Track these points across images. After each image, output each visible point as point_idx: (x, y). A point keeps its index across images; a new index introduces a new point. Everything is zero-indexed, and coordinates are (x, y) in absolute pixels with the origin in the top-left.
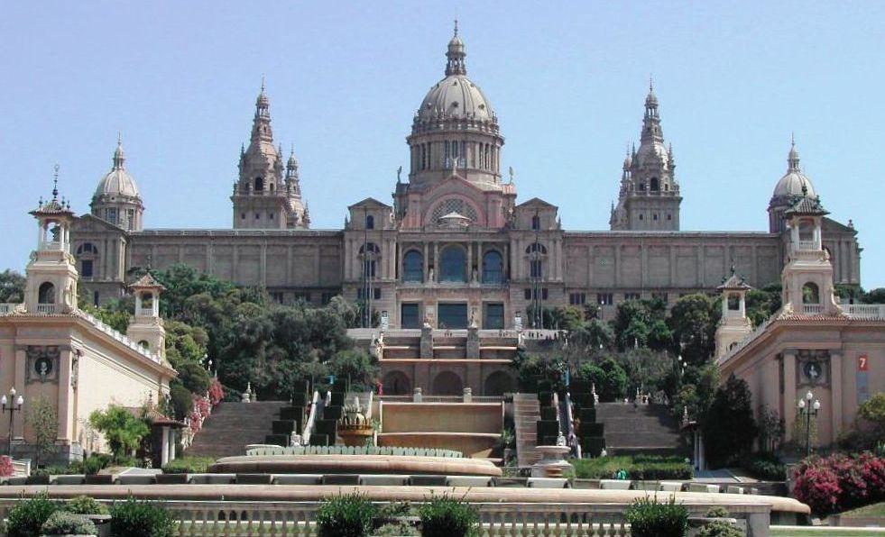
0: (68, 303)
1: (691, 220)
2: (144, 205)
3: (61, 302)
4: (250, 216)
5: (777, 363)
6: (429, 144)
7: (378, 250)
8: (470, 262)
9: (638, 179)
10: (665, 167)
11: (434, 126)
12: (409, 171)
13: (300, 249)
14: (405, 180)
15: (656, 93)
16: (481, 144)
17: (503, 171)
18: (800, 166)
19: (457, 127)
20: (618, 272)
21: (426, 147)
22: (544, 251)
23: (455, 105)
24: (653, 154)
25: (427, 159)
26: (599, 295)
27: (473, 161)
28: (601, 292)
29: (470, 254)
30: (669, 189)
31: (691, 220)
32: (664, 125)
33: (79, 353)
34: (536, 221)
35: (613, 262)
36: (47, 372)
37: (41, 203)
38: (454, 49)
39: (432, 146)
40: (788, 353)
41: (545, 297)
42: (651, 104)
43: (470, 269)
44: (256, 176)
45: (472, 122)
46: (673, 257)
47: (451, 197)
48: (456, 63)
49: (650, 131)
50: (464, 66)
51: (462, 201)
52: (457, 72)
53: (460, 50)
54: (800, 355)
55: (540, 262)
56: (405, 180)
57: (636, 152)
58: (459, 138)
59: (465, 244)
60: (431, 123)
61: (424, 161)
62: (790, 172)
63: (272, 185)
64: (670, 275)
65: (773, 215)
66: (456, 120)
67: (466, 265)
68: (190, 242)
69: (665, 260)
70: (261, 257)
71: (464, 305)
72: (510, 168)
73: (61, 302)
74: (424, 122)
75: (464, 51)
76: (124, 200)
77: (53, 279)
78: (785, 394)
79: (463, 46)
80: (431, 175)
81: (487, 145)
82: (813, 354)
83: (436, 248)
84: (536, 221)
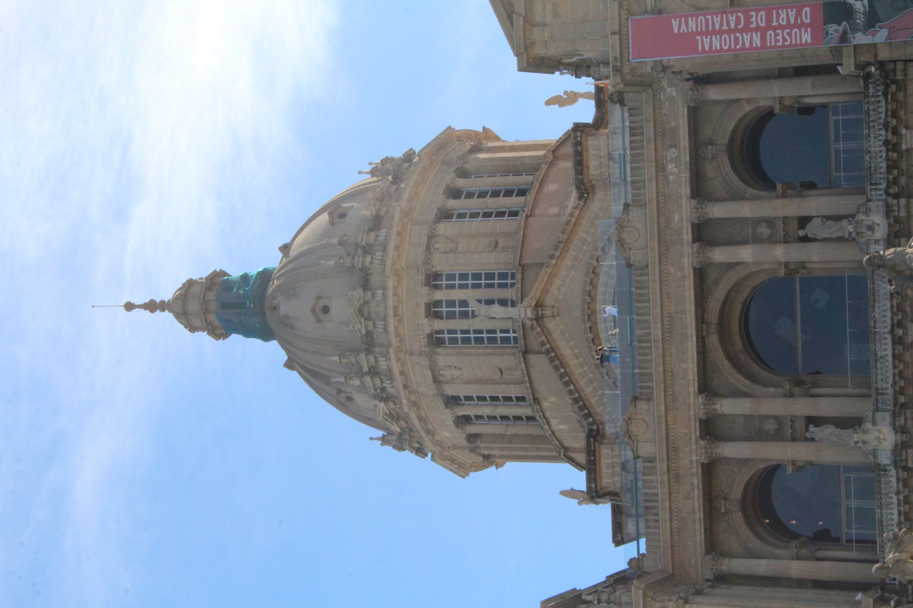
6: (452, 401)
11: (387, 384)
16: (445, 215)
29: (746, 254)
38: (194, 306)
39: (450, 391)
45: (367, 250)
50: (245, 278)
53: (196, 289)
60: (383, 396)
61: (518, 418)
67: (792, 269)
72: (549, 103)
74: (395, 417)
79: (190, 283)
81: (455, 193)
83: (727, 406)
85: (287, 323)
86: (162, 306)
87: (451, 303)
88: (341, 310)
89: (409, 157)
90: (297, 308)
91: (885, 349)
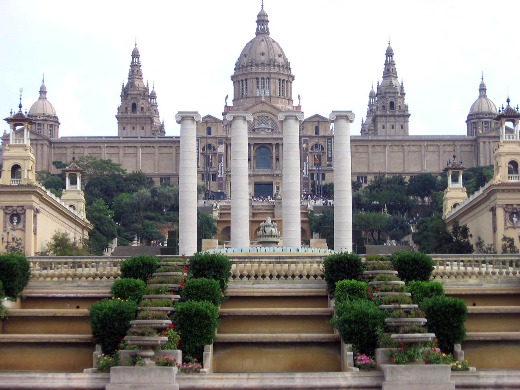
0: (30, 178)
1: (416, 128)
2: (59, 121)
3: (26, 177)
4: (129, 128)
5: (491, 214)
6: (246, 80)
7: (214, 149)
8: (274, 156)
9: (381, 102)
10: (399, 95)
12: (233, 99)
13: (163, 148)
14: (230, 104)
15: (393, 46)
16: (280, 80)
17: (294, 97)
18: (488, 93)
19: (264, 69)
20: (370, 163)
21: (244, 82)
22: (323, 149)
23: (263, 54)
24: (391, 84)
25: (244, 90)
26: (358, 178)
27: (275, 91)
28: (360, 175)
29: (274, 151)
30: (402, 108)
31: (416, 128)
32: (399, 67)
33: (37, 211)
34: (317, 131)
35: (367, 156)
36: (18, 223)
37: (11, 113)
38: (262, 18)
39: (248, 81)
40: (499, 206)
41: (323, 178)
42: (389, 53)
43: (274, 161)
44: (132, 102)
45: (274, 65)
46: (406, 153)
47: (261, 114)
48: (263, 27)
49: (389, 71)
50: (268, 29)
51: (268, 117)
52: (264, 33)
53: (266, 18)
54: (506, 207)
55: (320, 156)
56: (230, 104)
57: (380, 85)
58: (265, 76)
59: (271, 144)
60: (247, 66)
61: (243, 91)
62: (480, 97)
63: (142, 108)
64: (404, 164)
65: (470, 125)
66: (263, 64)
67: (272, 157)
68: (91, 145)
69: (401, 154)
70: (138, 155)
71: (271, 184)
73: (26, 177)
74: (243, 66)
75: (268, 19)
76: (47, 119)
77: (20, 163)
78: (496, 233)
79: (267, 16)
80: (248, 100)
82: (515, 206)
84: (317, 131)
85: (260, 43)
86: (262, 8)
87: (264, 82)
88: (263, 58)
89: (290, 69)
90: (263, 47)
91: (262, 173)
